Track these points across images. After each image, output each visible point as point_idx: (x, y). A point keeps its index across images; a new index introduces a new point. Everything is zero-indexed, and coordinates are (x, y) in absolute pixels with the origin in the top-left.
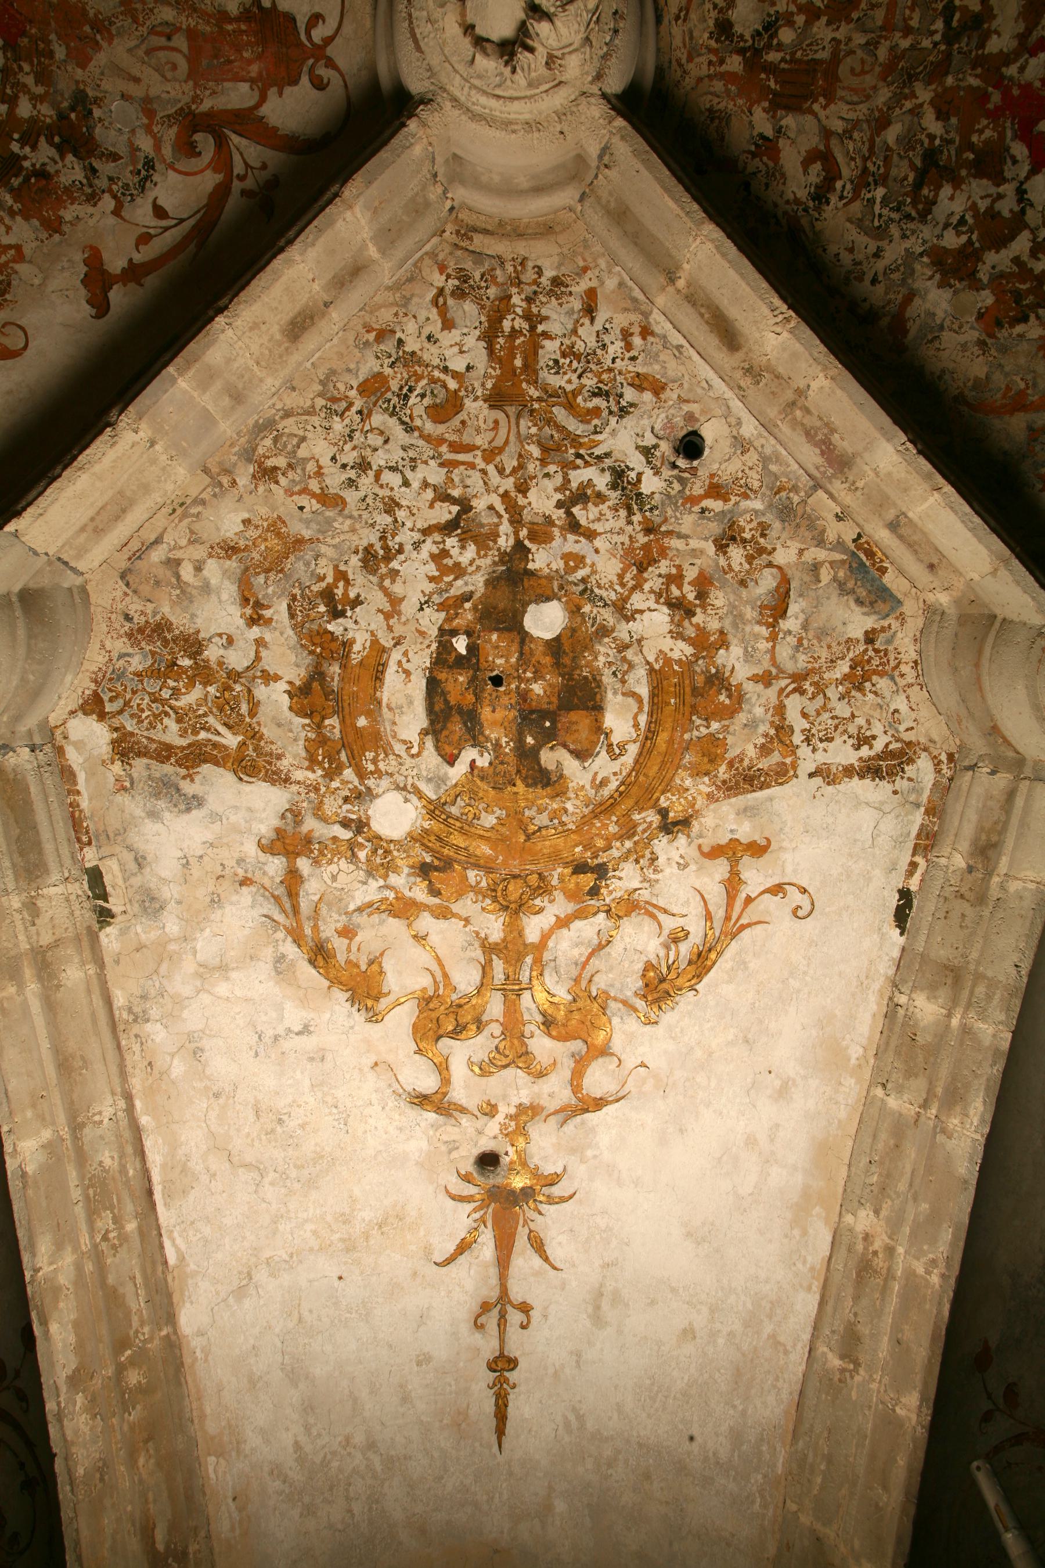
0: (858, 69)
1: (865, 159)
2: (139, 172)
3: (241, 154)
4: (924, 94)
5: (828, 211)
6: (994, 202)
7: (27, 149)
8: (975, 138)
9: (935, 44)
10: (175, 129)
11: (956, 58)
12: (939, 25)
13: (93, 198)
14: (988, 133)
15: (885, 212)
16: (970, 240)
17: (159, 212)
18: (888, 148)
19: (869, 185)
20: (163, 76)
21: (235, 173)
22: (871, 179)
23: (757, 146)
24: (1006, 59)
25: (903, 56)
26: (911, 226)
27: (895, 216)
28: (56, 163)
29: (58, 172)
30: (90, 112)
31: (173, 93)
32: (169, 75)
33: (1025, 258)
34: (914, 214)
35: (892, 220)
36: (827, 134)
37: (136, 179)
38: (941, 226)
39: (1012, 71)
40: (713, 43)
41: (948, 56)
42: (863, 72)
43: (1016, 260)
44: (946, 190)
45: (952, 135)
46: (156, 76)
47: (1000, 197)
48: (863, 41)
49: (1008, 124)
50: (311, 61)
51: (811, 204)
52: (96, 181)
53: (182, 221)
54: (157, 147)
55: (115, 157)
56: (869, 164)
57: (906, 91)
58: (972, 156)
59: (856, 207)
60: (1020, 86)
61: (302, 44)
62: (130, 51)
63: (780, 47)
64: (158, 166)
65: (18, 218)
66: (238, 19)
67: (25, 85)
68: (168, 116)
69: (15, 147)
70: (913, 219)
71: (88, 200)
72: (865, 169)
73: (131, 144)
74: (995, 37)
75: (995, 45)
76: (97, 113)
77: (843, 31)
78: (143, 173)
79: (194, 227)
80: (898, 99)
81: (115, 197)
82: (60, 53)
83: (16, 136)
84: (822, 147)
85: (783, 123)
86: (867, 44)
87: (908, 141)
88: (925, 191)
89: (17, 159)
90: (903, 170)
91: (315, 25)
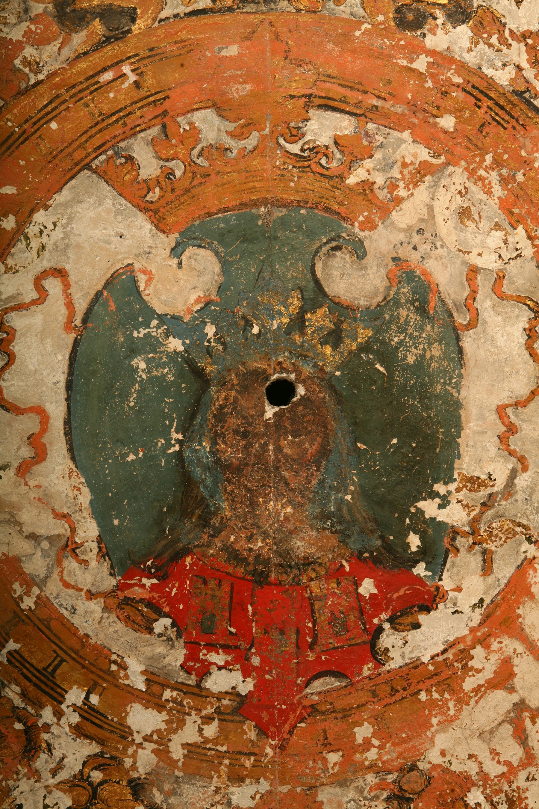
7: (75, 719)
28: (54, 773)
29: (36, 775)
67: (182, 723)
83: (94, 699)
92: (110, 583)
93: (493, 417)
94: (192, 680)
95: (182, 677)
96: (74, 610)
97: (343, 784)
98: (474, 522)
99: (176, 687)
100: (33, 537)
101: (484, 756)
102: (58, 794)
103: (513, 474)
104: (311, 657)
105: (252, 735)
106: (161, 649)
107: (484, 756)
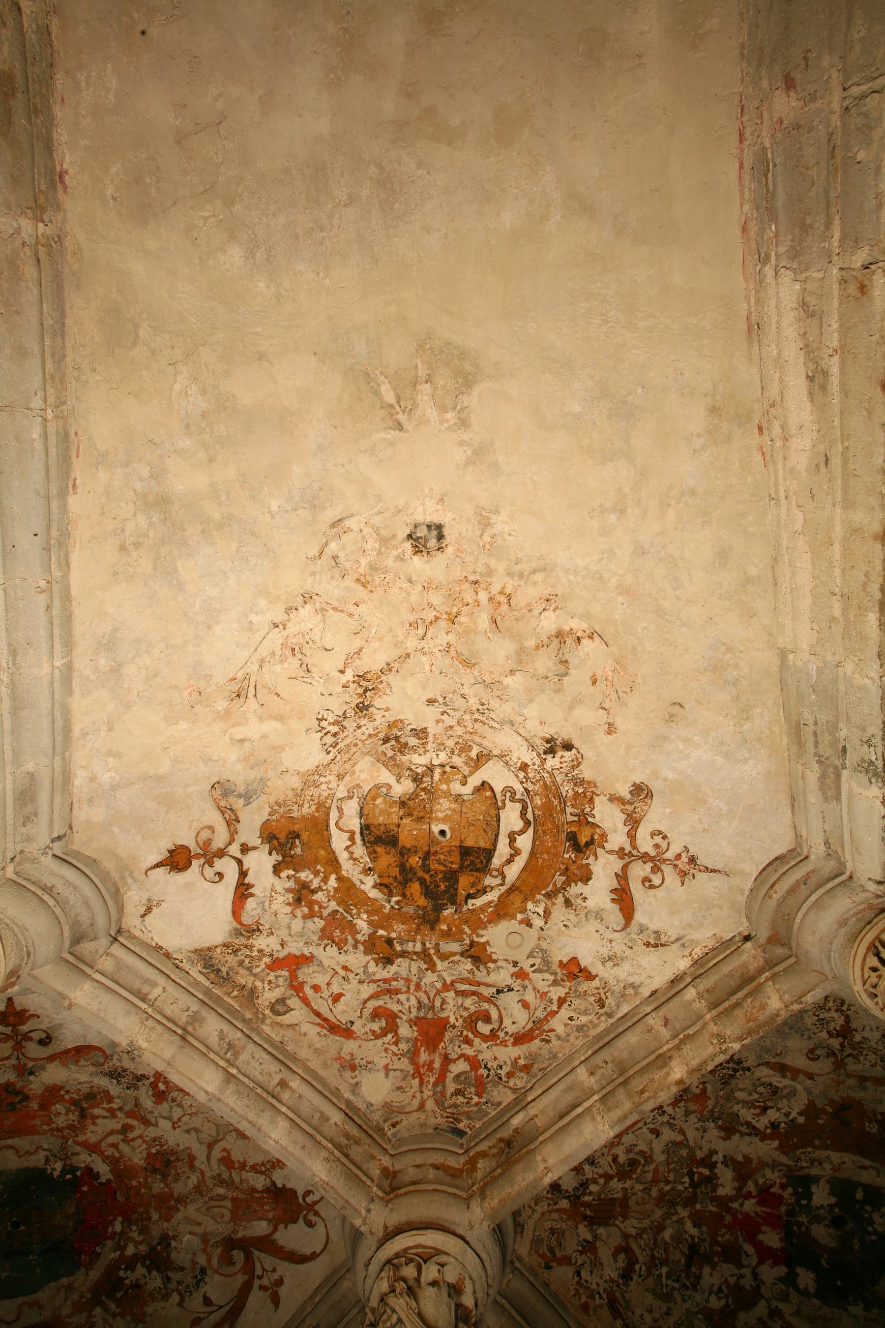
0: (640, 1201)
1: (652, 1250)
2: (196, 1276)
3: (261, 1262)
4: (684, 1213)
5: (633, 1285)
6: (738, 1279)
8: (720, 1239)
9: (686, 1188)
10: (220, 1249)
11: (700, 1196)
12: (686, 1179)
13: (166, 1297)
14: (727, 1237)
15: (669, 1282)
16: (727, 1302)
17: (207, 1301)
18: (666, 1243)
19: (656, 1265)
20: (216, 1221)
21: (256, 1274)
22: (657, 1262)
23: (583, 1247)
24: (731, 1199)
25: (667, 1192)
26: (687, 1292)
27: (676, 1285)
28: (145, 1277)
29: (146, 1283)
30: (170, 1244)
31: (221, 1229)
32: (219, 1220)
33: (765, 1319)
34: (688, 1284)
35: (674, 1288)
36: (626, 1236)
37: (194, 1281)
38: (707, 1293)
39: (735, 1205)
40: (550, 1195)
41: (695, 1195)
42: (644, 1203)
43: (760, 1319)
44: (707, 1270)
45: (705, 1236)
46: (212, 1221)
47: (742, 1276)
48: (641, 1187)
49: (739, 1233)
50: (305, 1212)
51: (621, 1281)
52: (170, 1285)
53: (221, 1307)
54: (209, 1260)
55: (182, 1269)
56: (655, 1253)
57: (672, 1211)
58: (719, 1249)
59: (650, 1281)
60: (742, 1213)
61: (300, 1204)
62: (197, 1210)
63: (591, 1193)
64: (209, 1272)
65: (118, 1318)
66: (262, 1192)
67: (132, 1238)
68: (217, 1242)
69: (122, 1273)
70: (688, 1288)
71: (163, 1298)
72: (653, 1256)
73: (193, 1260)
74: (721, 1188)
75: (721, 1191)
76: (174, 1244)
77: (628, 1184)
78: (199, 1277)
79: (229, 1312)
80: (668, 1215)
81: (180, 1294)
82: (155, 1216)
83: (123, 1267)
84: (624, 1244)
85: (598, 1232)
86: (644, 1189)
87: (678, 1238)
88: (693, 1269)
89: (123, 1279)
90: (677, 1256)
91: (308, 1195)
92: (83, 1269)
93: (23, 1159)
94: (118, 1237)
95: (116, 1240)
96: (92, 1280)
97: (151, 1187)
98: (61, 1159)
99: (120, 1241)
100: (65, 1300)
101: (140, 1149)
102: (152, 1276)
103: (44, 1150)
104: (109, 1202)
105: (136, 1215)
106: (107, 1248)
107: (140, 1149)
